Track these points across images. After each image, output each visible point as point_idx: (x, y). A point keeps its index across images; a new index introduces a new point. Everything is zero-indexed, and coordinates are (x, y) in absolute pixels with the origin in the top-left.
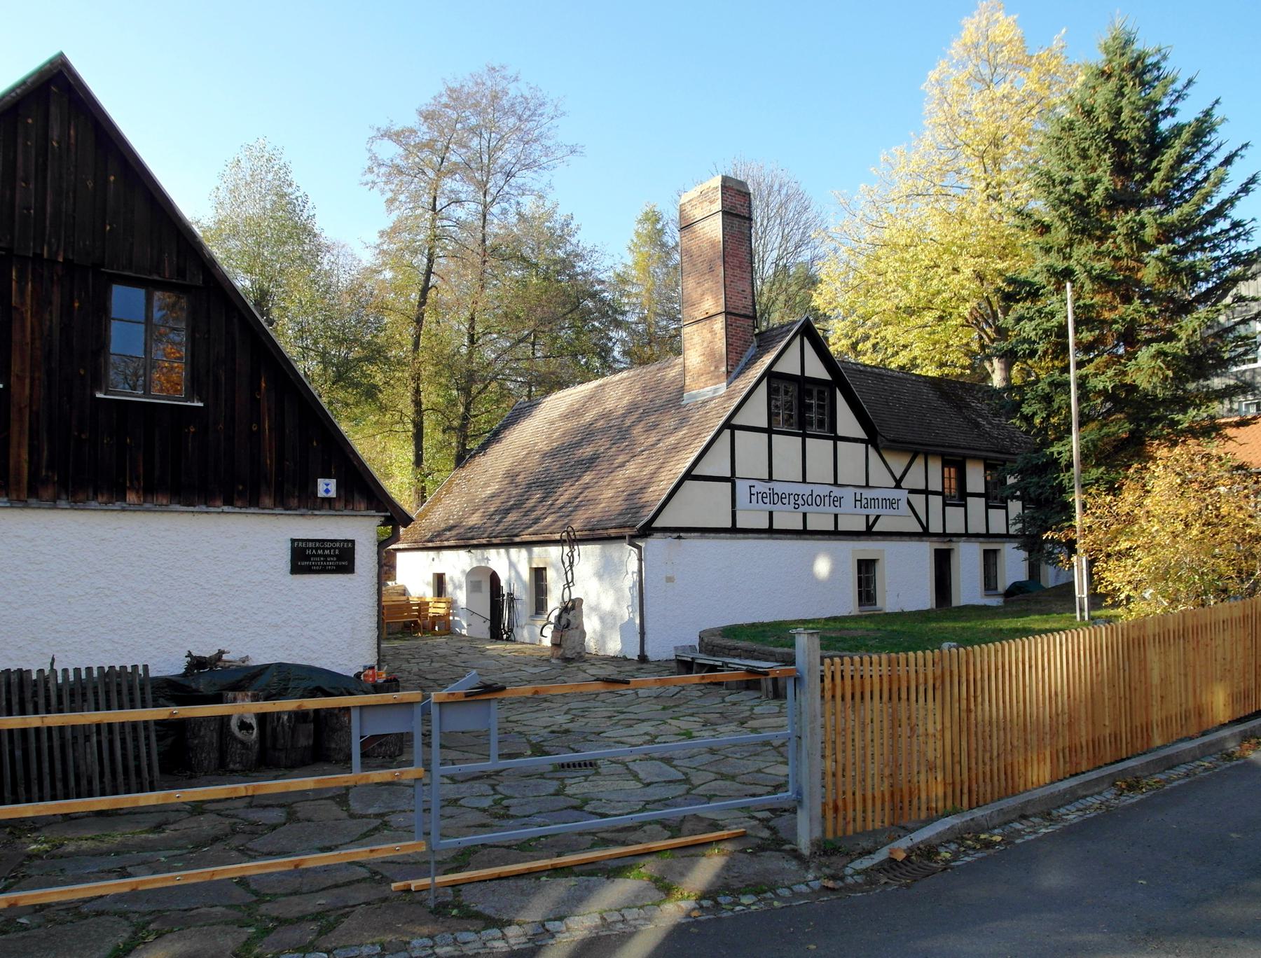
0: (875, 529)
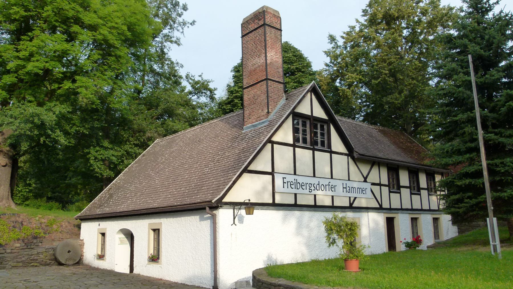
0: (354, 205)
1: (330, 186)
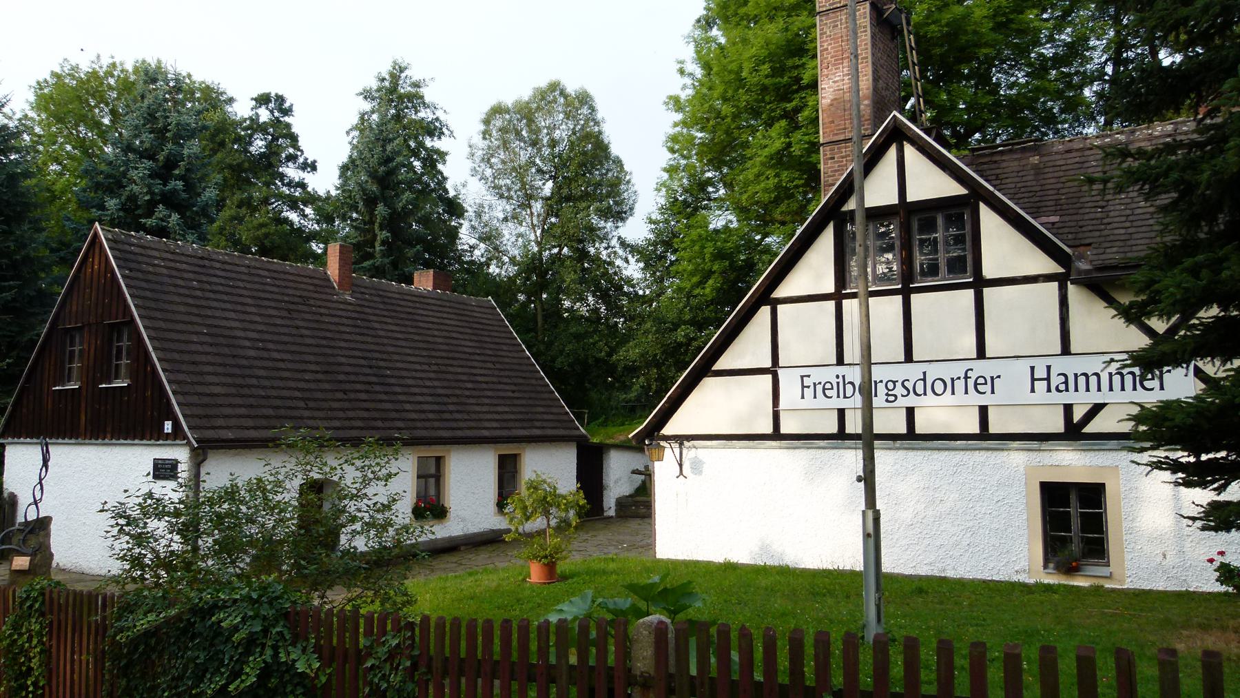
1: (971, 383)
